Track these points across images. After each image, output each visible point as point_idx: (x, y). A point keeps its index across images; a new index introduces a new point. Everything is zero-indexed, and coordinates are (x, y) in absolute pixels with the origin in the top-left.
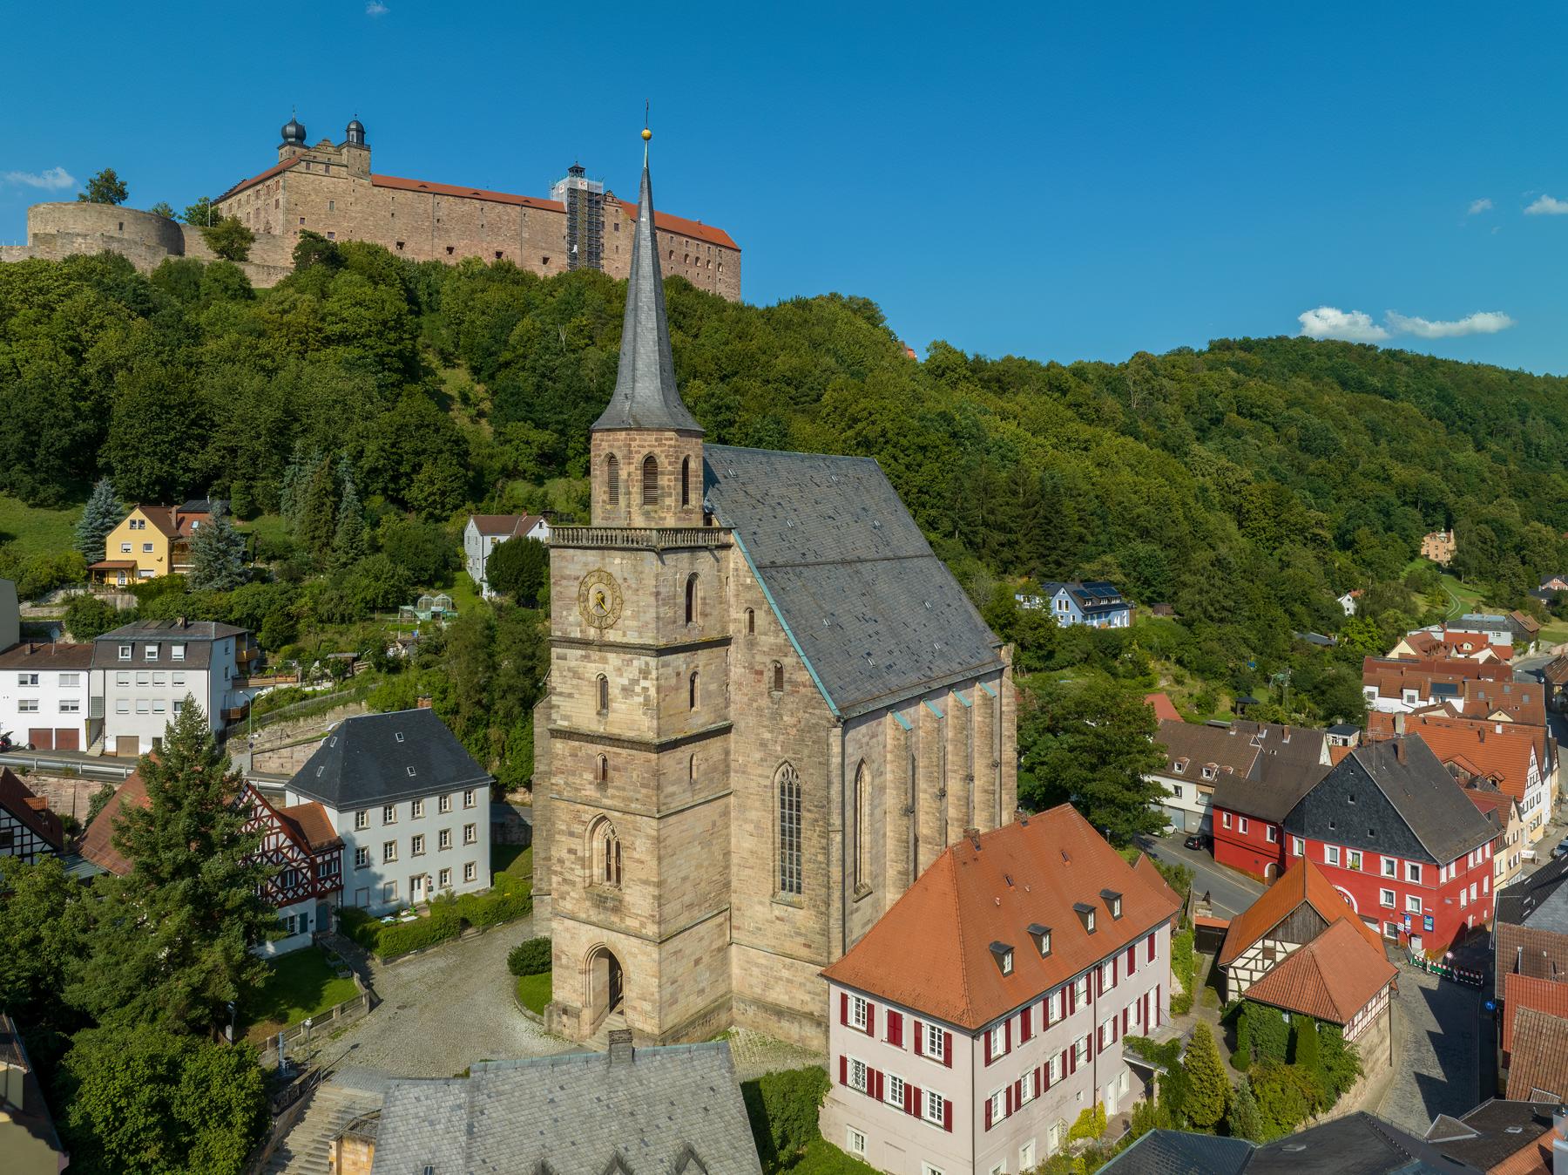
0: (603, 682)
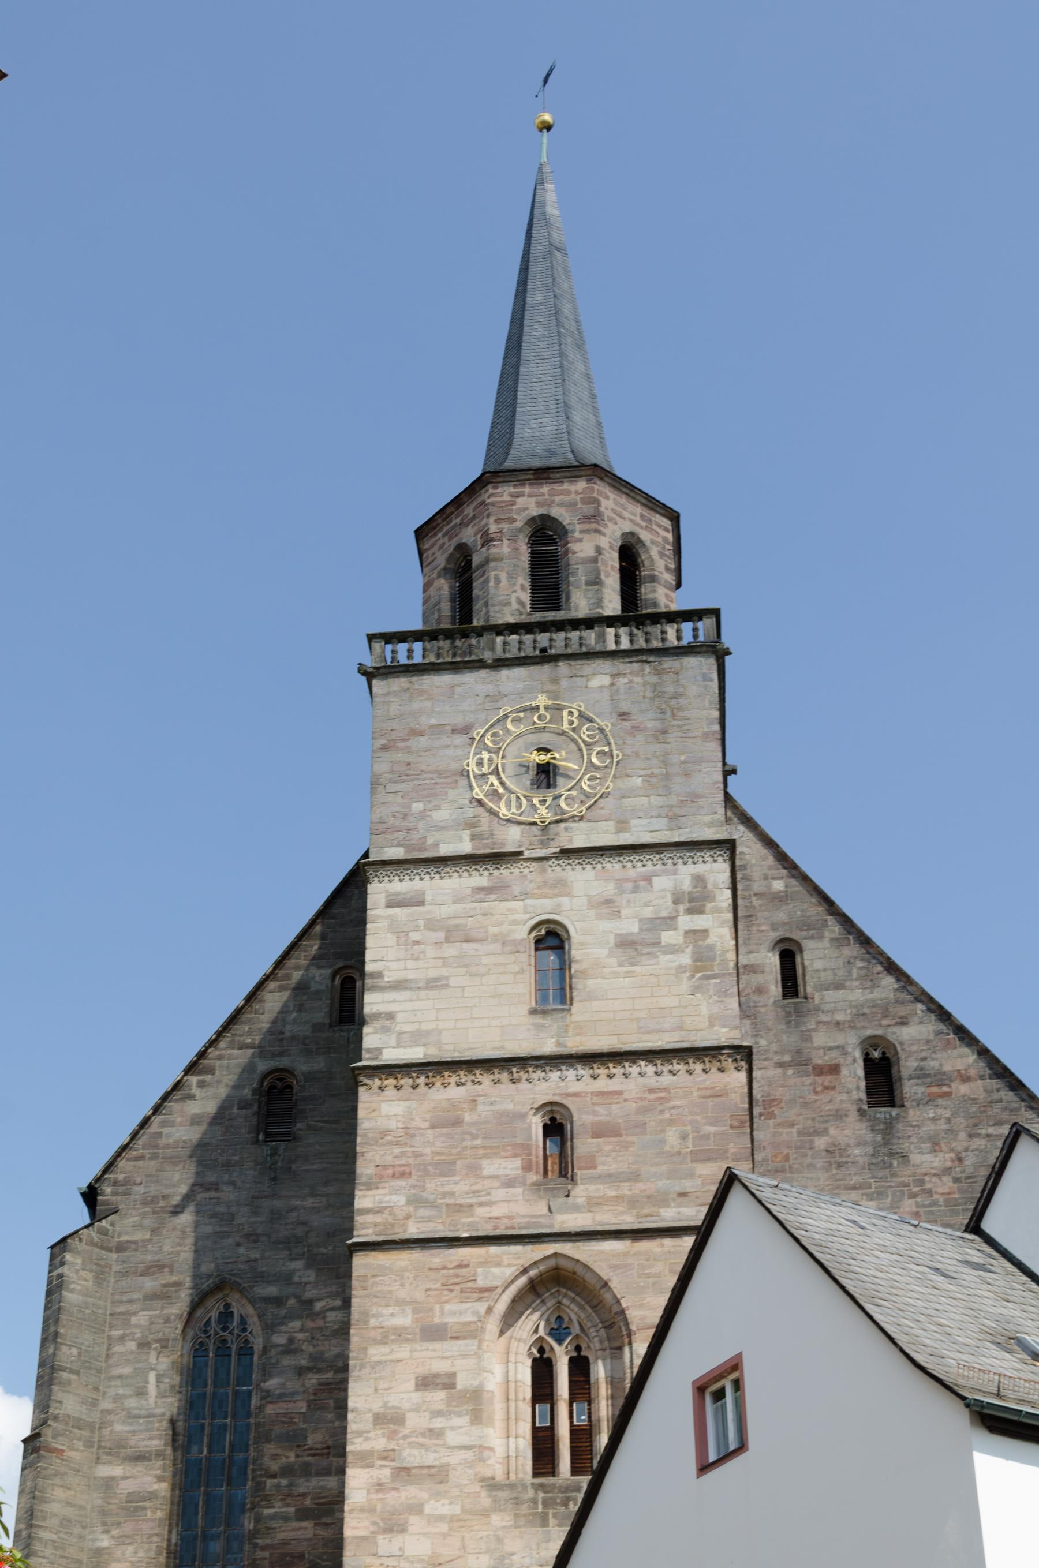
0: (551, 939)
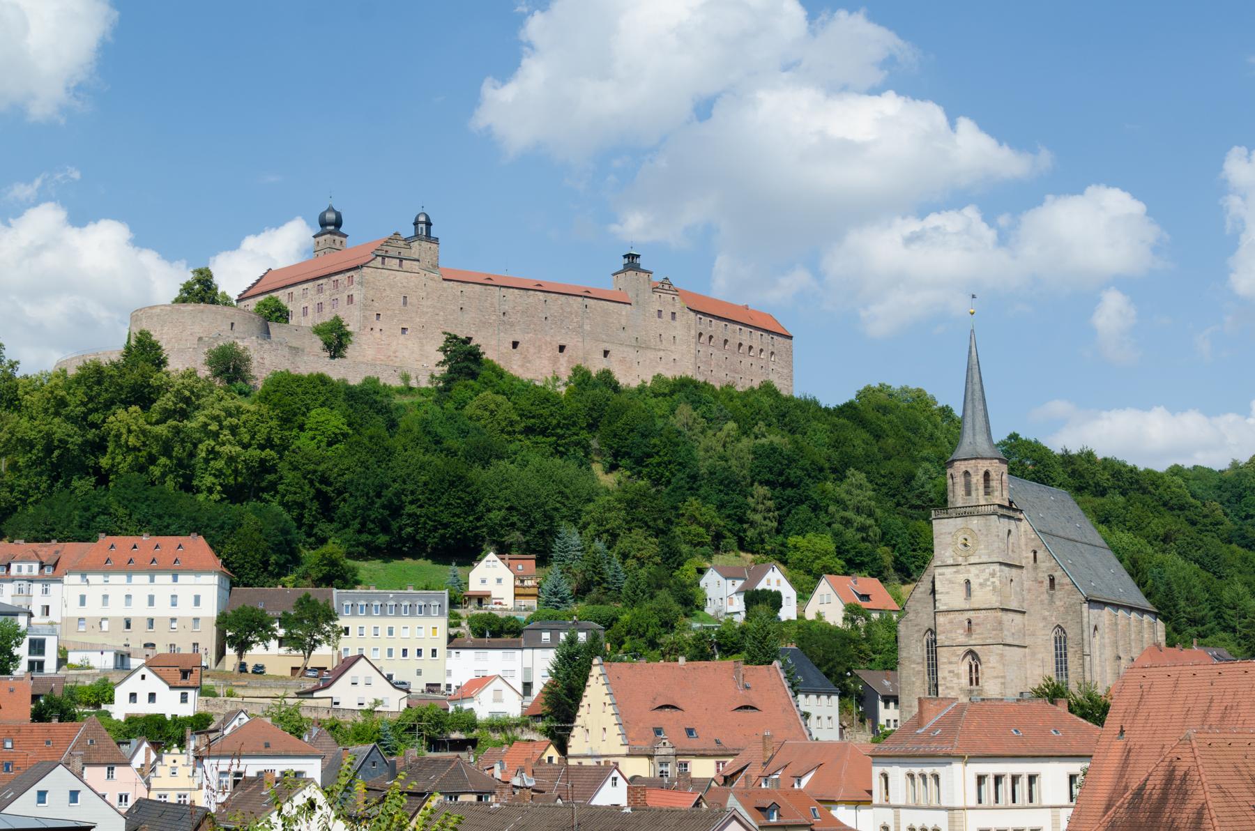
0: (968, 582)
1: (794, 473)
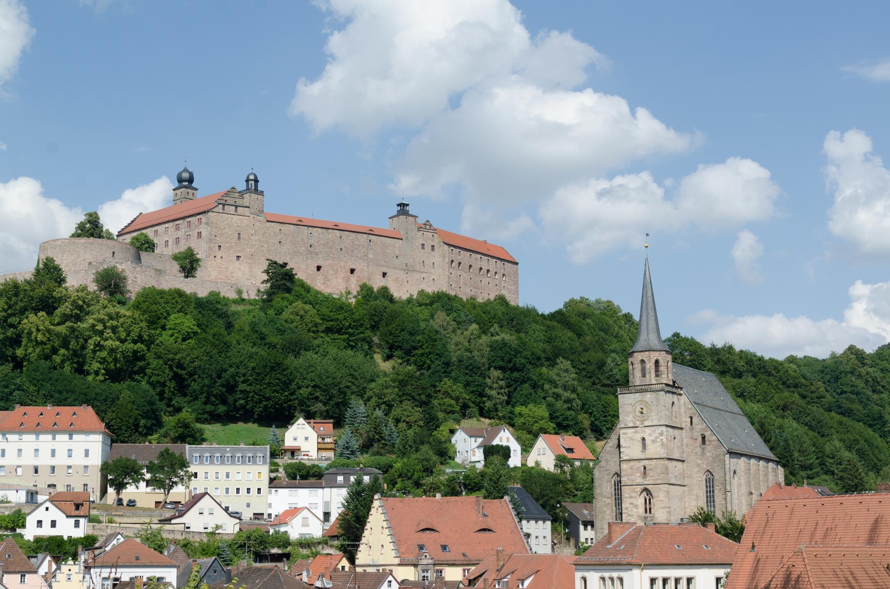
0: (644, 439)
1: (519, 361)
